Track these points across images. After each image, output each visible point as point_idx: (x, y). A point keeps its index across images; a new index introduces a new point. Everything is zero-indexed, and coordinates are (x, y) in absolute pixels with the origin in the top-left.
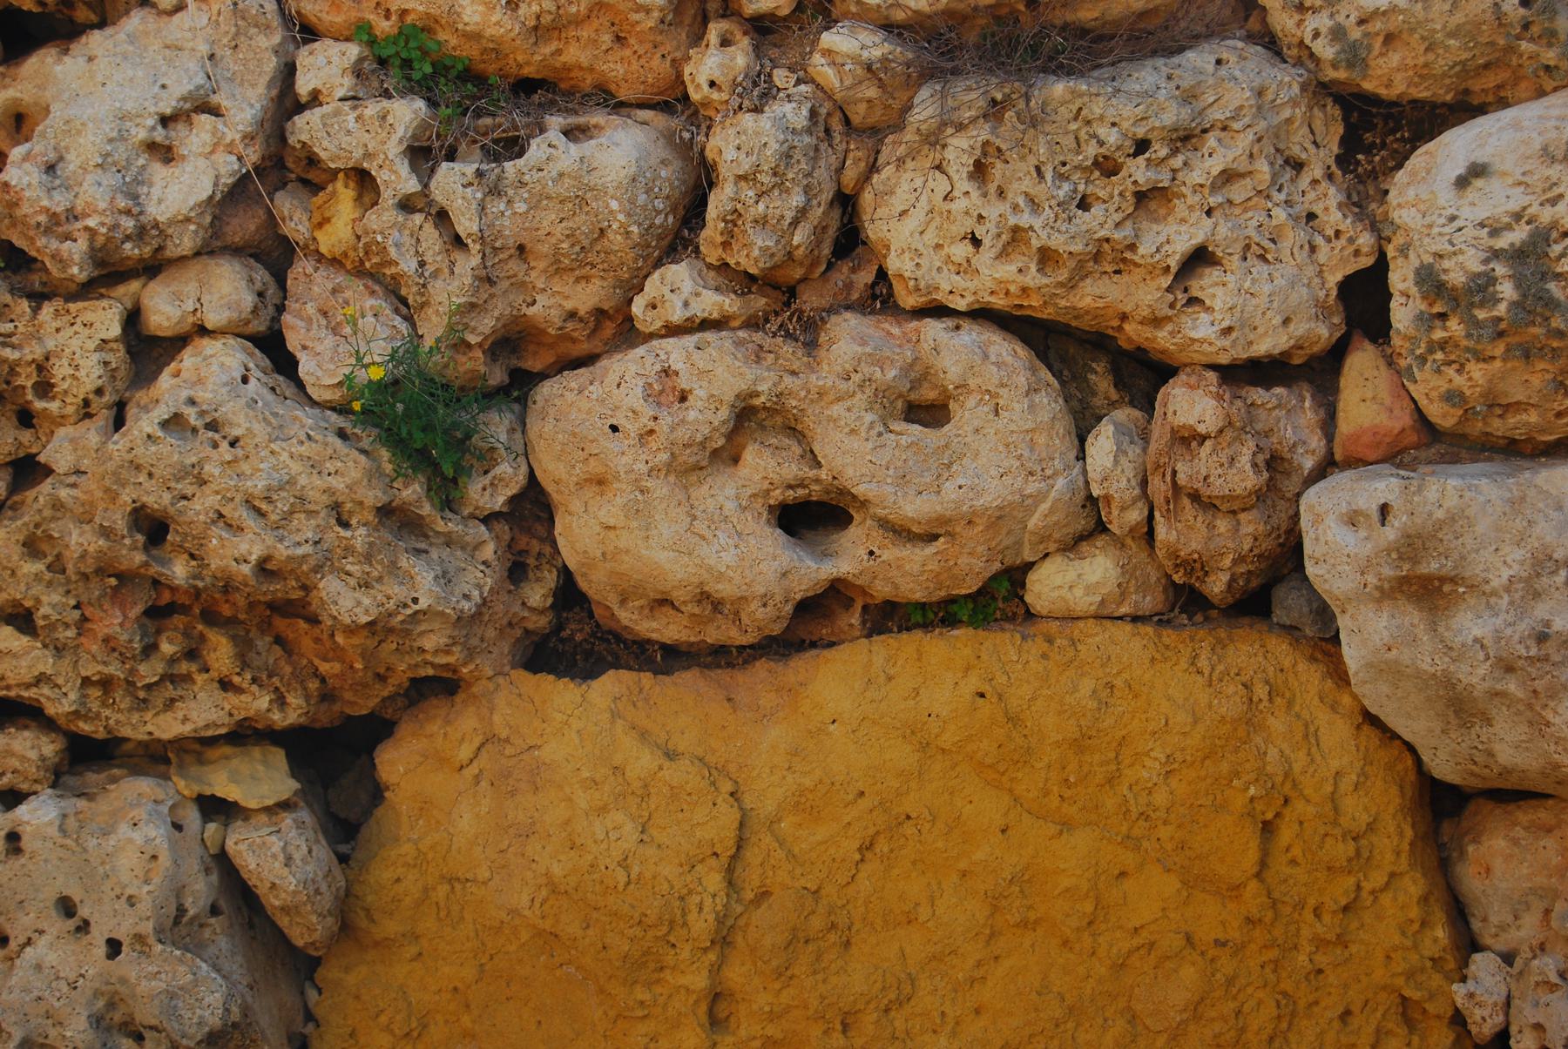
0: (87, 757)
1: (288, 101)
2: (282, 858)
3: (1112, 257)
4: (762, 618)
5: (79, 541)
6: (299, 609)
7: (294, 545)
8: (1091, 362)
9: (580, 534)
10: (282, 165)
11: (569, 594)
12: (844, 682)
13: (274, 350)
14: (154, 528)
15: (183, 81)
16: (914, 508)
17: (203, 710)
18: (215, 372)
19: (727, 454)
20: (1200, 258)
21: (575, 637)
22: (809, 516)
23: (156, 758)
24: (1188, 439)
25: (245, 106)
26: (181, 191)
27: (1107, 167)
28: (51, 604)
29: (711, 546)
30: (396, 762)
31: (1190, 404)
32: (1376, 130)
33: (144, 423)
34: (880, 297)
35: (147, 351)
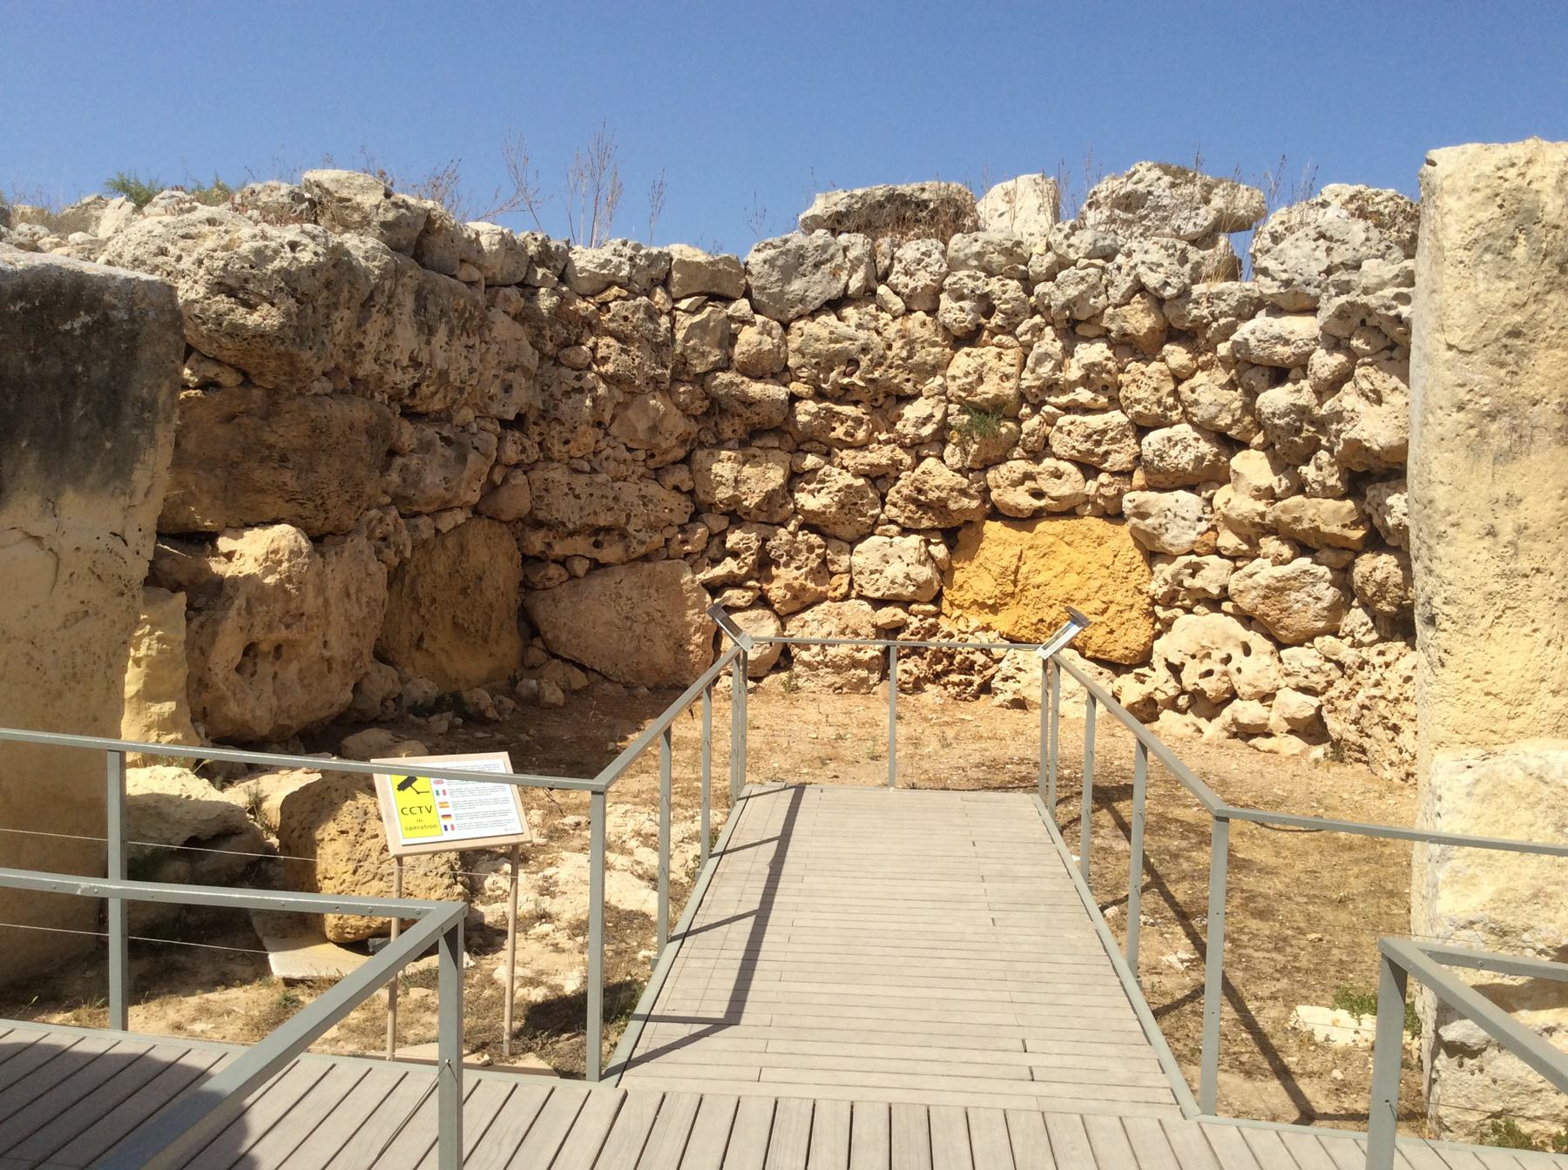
0: (905, 531)
1: (946, 415)
2: (940, 551)
3: (1090, 453)
4: (1027, 514)
5: (905, 491)
6: (946, 507)
7: (943, 495)
8: (1089, 469)
9: (994, 495)
10: (944, 427)
11: (994, 507)
12: (1042, 526)
13: (941, 458)
14: (920, 491)
15: (928, 411)
16: (1054, 494)
17: (925, 524)
18: (930, 463)
19: (1022, 483)
20: (1107, 453)
21: (996, 513)
22: (1037, 494)
23: (917, 532)
24: (1102, 485)
25: (938, 416)
26: (927, 430)
27: (1090, 436)
28: (900, 503)
29: (1021, 499)
30: (960, 535)
31: (1104, 478)
32: (1141, 429)
33: (918, 471)
34: (1054, 455)
35: (919, 459)
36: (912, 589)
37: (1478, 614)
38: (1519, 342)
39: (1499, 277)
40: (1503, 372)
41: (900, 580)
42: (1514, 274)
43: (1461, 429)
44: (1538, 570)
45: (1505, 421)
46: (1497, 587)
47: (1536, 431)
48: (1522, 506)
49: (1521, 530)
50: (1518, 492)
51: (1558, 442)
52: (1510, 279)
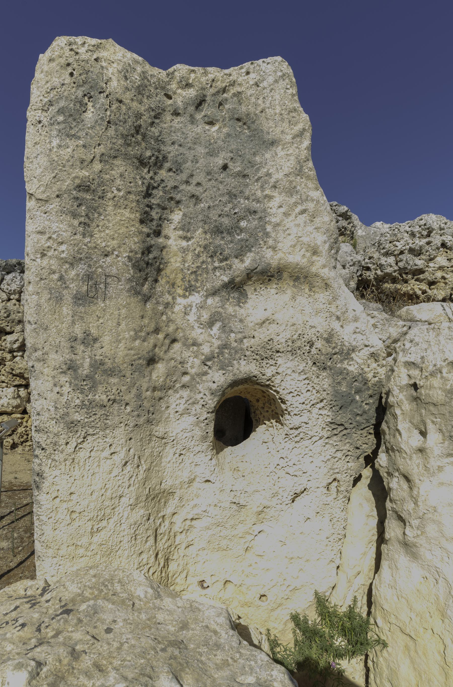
36: (11, 408)
37: (62, 442)
38: (88, 196)
39: (68, 136)
40: (76, 223)
41: (6, 405)
42: (81, 134)
43: (45, 273)
44: (114, 401)
45: (81, 269)
46: (77, 417)
47: (109, 280)
48: (97, 345)
49: (97, 365)
50: (94, 332)
51: (129, 291)
52: (79, 138)
